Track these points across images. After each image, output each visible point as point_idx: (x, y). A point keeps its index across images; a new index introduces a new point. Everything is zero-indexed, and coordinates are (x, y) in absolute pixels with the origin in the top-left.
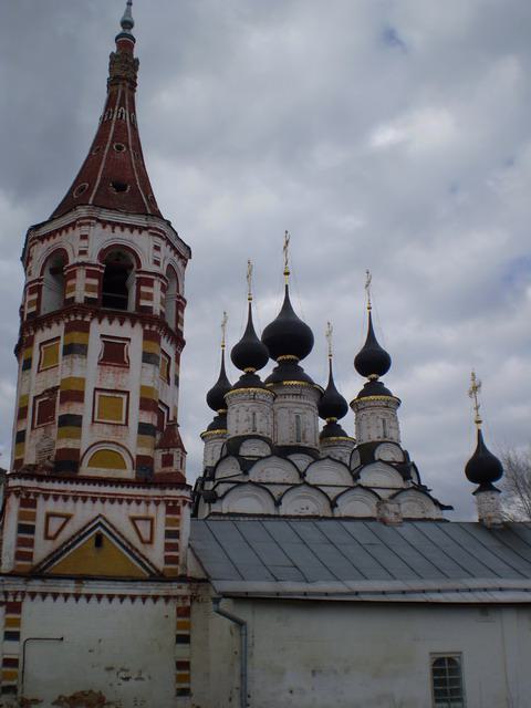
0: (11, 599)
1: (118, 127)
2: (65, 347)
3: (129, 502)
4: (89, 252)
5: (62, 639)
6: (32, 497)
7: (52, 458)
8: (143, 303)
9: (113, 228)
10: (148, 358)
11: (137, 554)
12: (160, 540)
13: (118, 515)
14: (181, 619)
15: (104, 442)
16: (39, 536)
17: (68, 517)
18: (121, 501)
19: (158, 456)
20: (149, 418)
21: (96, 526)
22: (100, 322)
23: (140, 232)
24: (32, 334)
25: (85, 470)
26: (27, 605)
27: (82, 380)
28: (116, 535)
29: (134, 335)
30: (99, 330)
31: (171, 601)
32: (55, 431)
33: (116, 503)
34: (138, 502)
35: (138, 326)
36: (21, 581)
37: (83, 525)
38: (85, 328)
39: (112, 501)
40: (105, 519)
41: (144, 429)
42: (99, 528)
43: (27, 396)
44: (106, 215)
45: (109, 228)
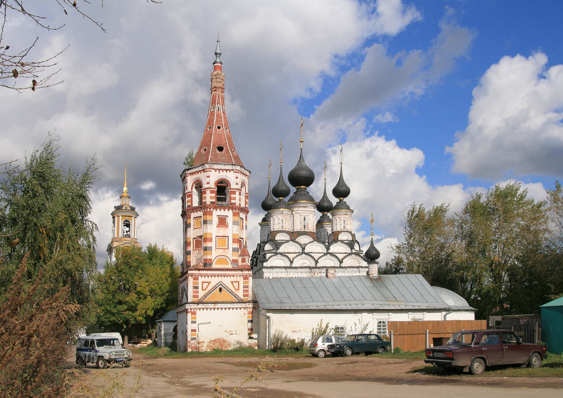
1: (218, 116)
2: (204, 221)
3: (230, 276)
4: (211, 183)
6: (197, 277)
8: (232, 201)
9: (219, 172)
10: (234, 223)
12: (241, 289)
13: (227, 281)
15: (220, 255)
16: (200, 289)
17: (209, 283)
18: (227, 276)
19: (240, 259)
20: (236, 246)
21: (219, 285)
22: (216, 210)
23: (230, 172)
25: (214, 266)
29: (229, 213)
30: (217, 213)
34: (234, 276)
35: (231, 210)
36: (195, 305)
37: (215, 285)
38: (211, 214)
39: (224, 276)
40: (222, 283)
41: (234, 250)
42: (220, 286)
44: (216, 167)
45: (217, 171)
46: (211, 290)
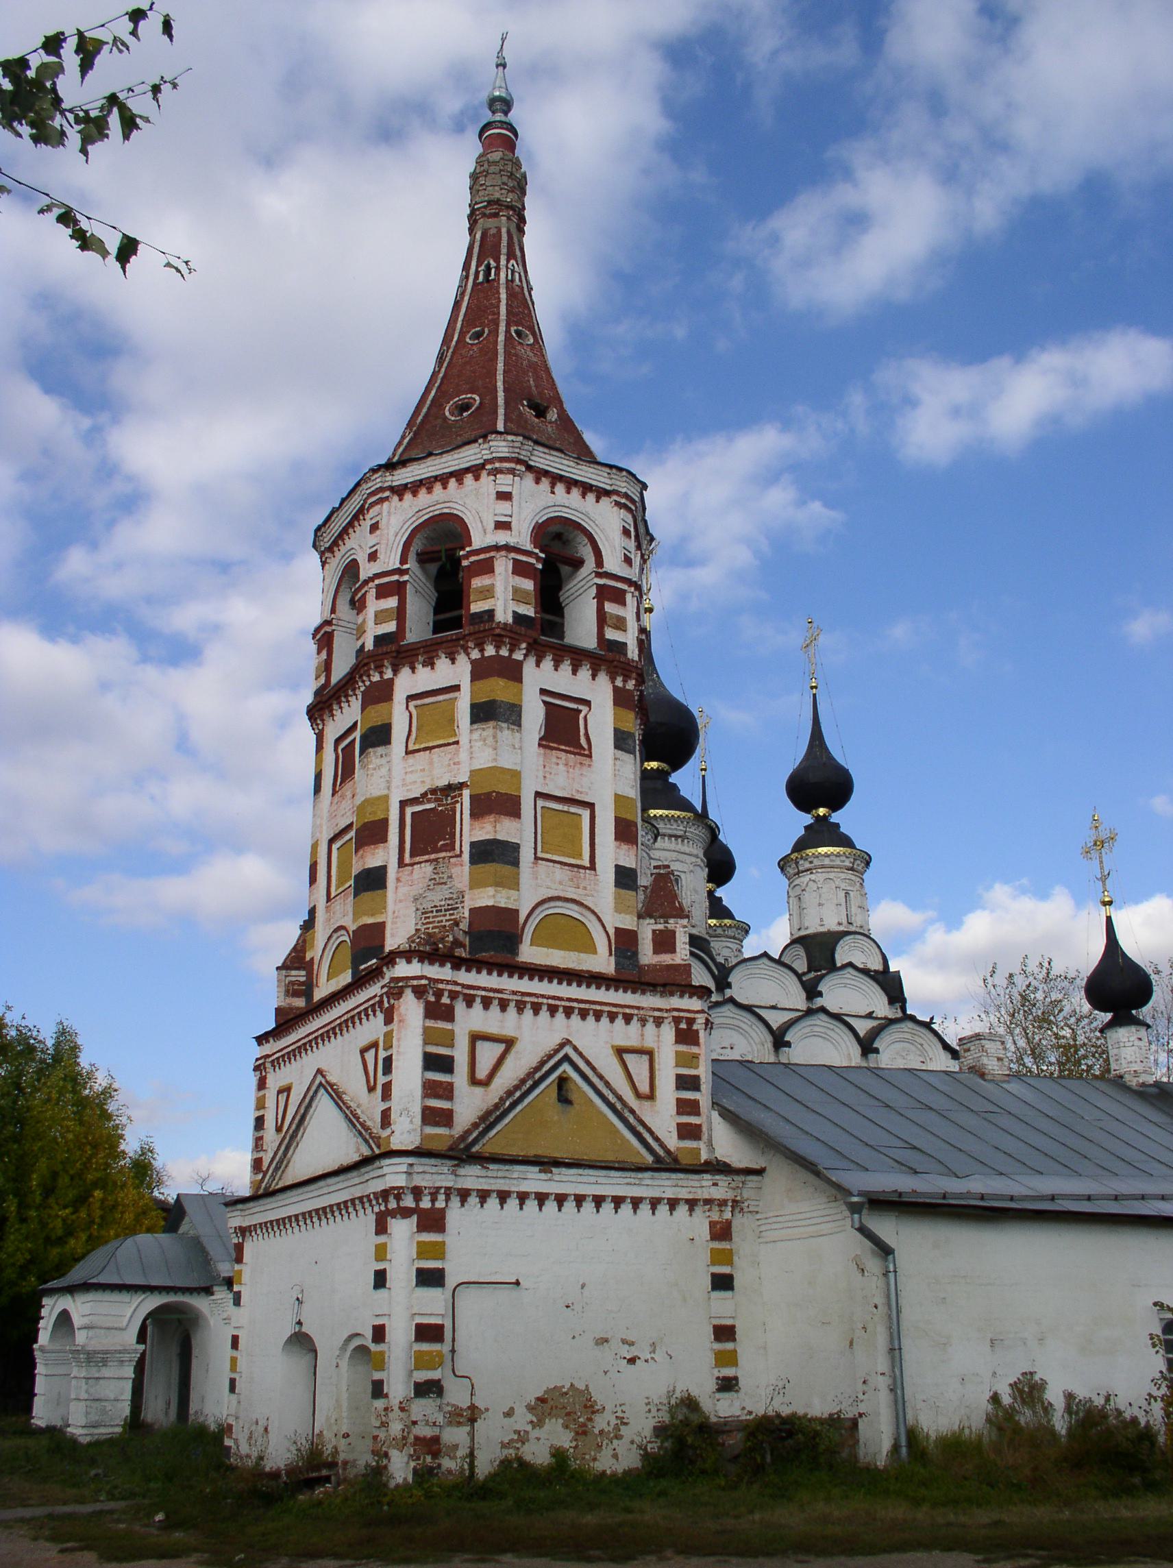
0: (426, 1204)
1: (512, 295)
2: (473, 706)
5: (517, 1283)
6: (445, 1000)
7: (464, 925)
8: (611, 634)
9: (553, 486)
11: (631, 1119)
14: (717, 1245)
15: (558, 898)
17: (509, 1043)
19: (647, 930)
24: (389, 674)
25: (529, 953)
26: (456, 1215)
27: (516, 775)
28: (595, 1080)
31: (698, 1210)
32: (461, 871)
33: (591, 1019)
36: (445, 1166)
38: (513, 672)
40: (575, 1049)
42: (566, 1067)
43: (385, 799)
45: (545, 482)
46: (517, 1088)
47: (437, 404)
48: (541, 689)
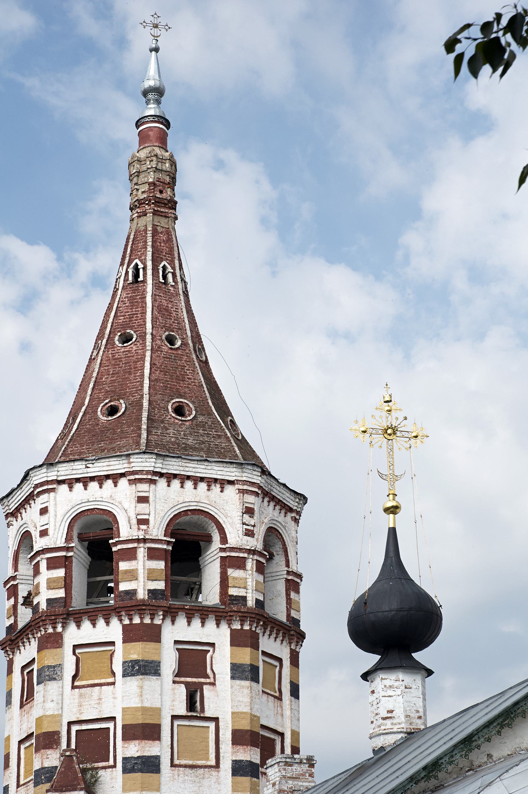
22: (173, 622)
24: (59, 629)
47: (92, 408)
48: (175, 641)
